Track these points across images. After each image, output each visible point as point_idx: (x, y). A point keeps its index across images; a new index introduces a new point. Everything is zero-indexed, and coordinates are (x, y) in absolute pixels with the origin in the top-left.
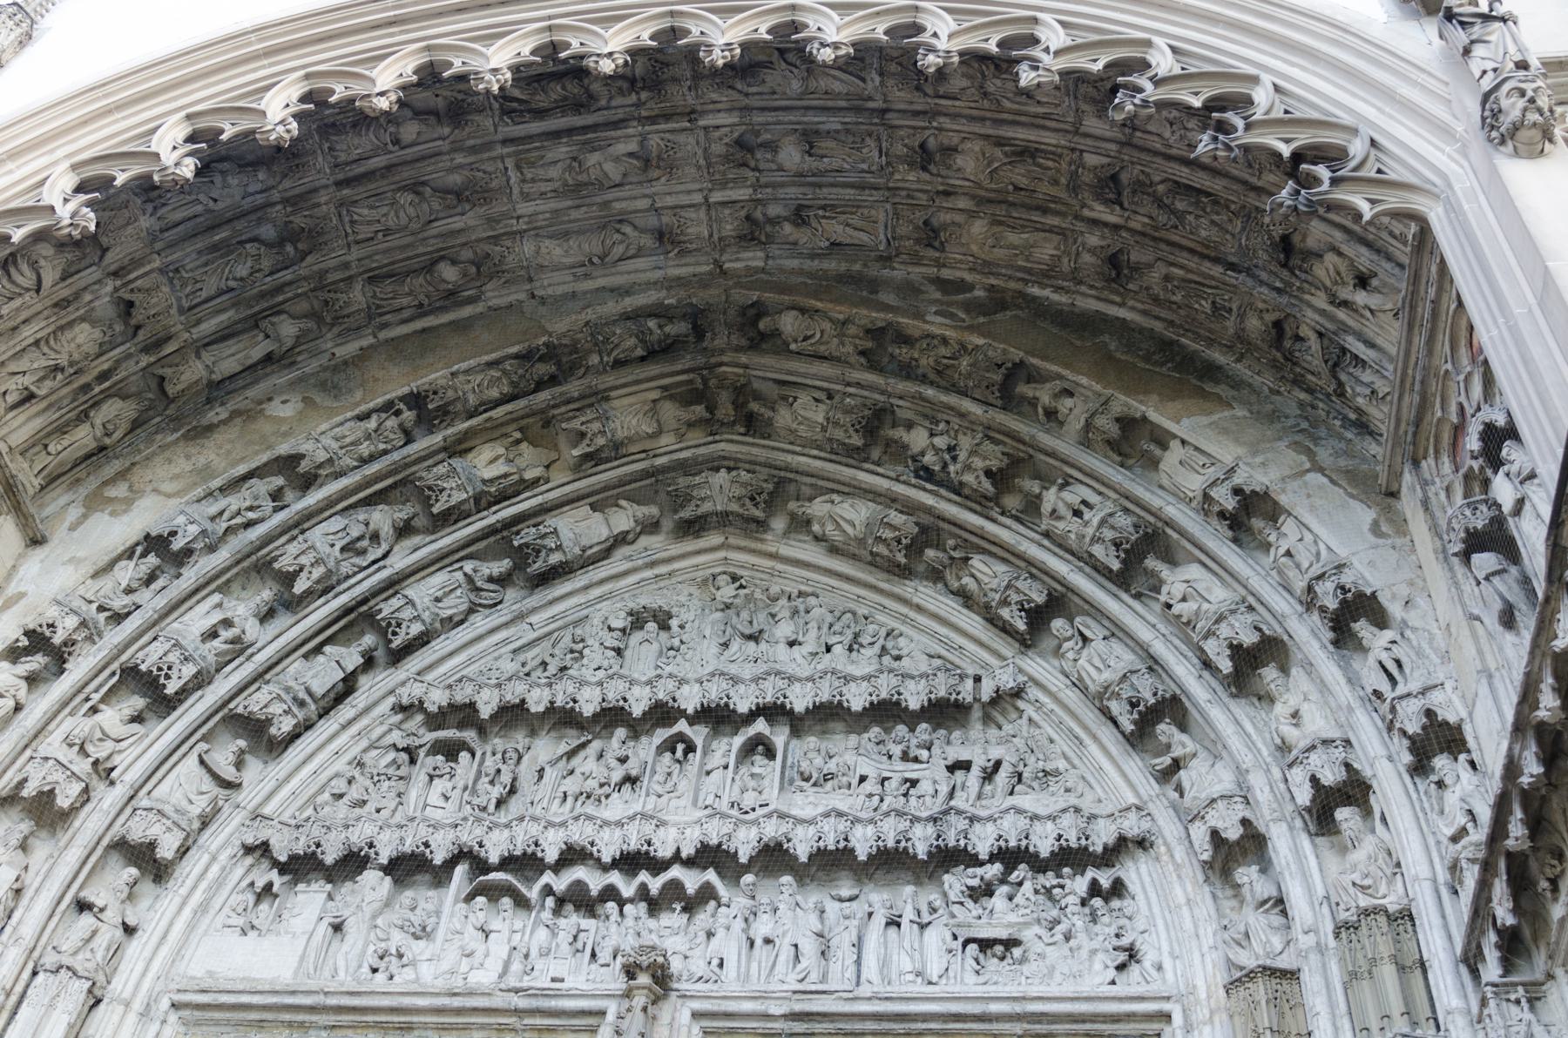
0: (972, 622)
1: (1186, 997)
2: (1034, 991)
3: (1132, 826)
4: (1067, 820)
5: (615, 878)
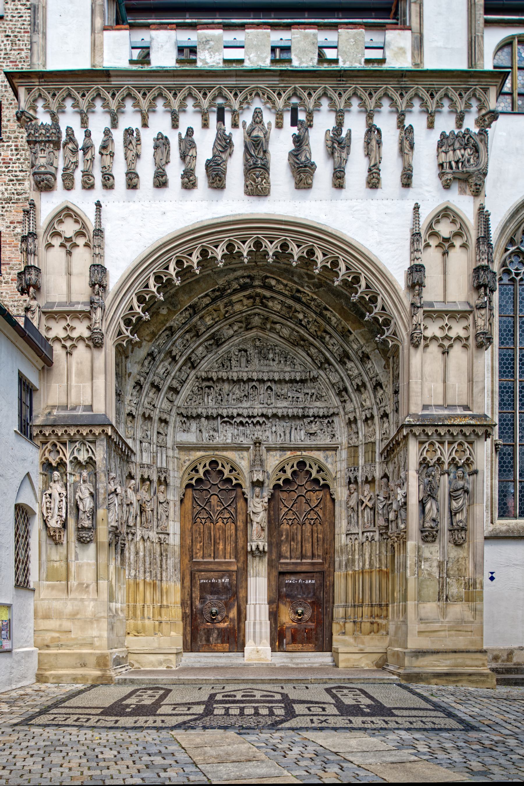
0: (309, 359)
1: (341, 444)
2: (319, 443)
3: (336, 410)
4: (325, 409)
5: (247, 419)
